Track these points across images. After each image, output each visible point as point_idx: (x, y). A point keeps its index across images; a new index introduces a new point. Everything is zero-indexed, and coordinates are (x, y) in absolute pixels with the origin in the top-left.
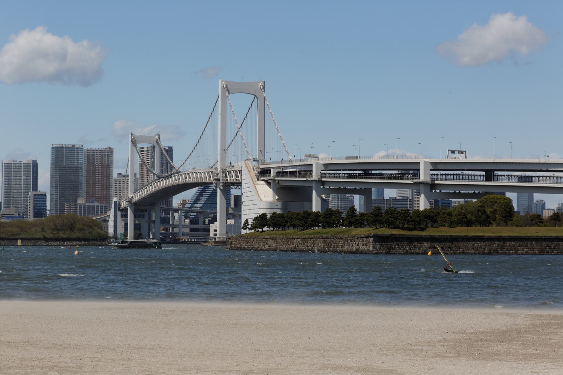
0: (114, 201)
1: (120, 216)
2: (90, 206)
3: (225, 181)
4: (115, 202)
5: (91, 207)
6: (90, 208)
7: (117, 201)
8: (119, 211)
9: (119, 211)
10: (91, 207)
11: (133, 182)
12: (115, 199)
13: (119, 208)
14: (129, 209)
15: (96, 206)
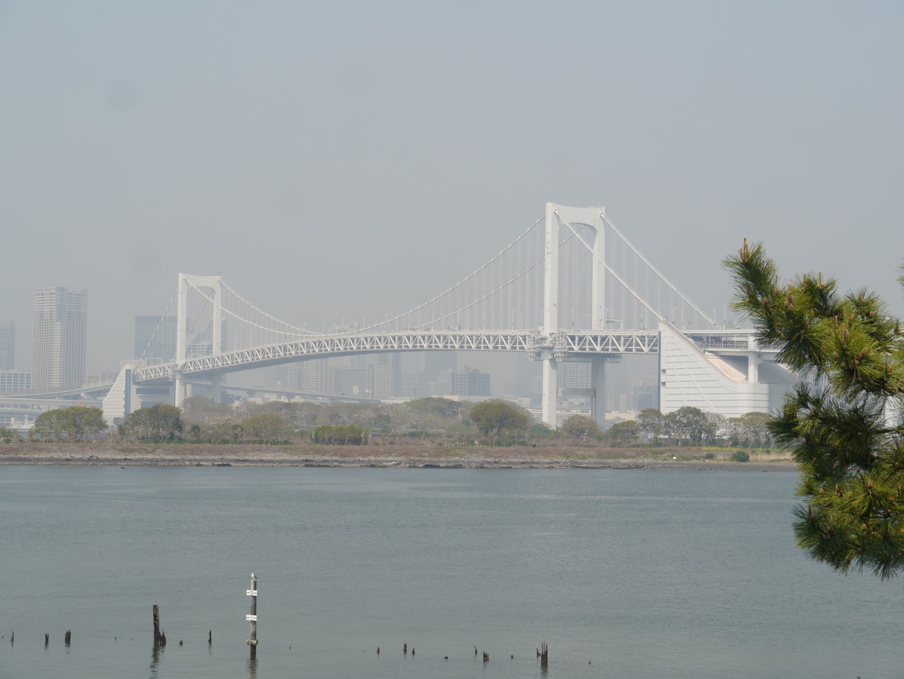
0: (127, 370)
1: (135, 392)
2: (5, 374)
3: (566, 350)
4: (128, 372)
5: (13, 375)
6: (24, 377)
7: (130, 370)
8: (133, 384)
9: (133, 384)
10: (25, 376)
11: (184, 343)
12: (128, 367)
13: (134, 380)
14: (177, 382)
15: (21, 374)
